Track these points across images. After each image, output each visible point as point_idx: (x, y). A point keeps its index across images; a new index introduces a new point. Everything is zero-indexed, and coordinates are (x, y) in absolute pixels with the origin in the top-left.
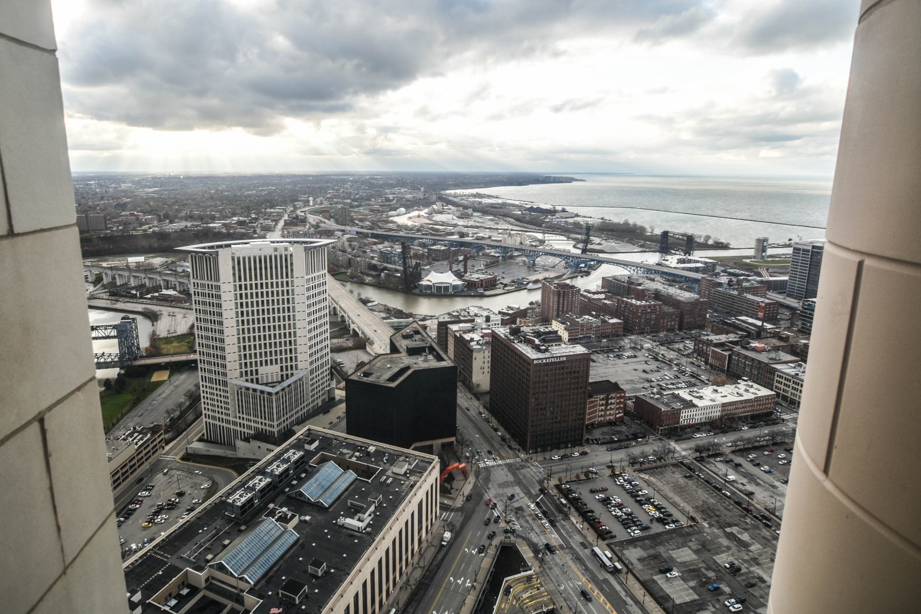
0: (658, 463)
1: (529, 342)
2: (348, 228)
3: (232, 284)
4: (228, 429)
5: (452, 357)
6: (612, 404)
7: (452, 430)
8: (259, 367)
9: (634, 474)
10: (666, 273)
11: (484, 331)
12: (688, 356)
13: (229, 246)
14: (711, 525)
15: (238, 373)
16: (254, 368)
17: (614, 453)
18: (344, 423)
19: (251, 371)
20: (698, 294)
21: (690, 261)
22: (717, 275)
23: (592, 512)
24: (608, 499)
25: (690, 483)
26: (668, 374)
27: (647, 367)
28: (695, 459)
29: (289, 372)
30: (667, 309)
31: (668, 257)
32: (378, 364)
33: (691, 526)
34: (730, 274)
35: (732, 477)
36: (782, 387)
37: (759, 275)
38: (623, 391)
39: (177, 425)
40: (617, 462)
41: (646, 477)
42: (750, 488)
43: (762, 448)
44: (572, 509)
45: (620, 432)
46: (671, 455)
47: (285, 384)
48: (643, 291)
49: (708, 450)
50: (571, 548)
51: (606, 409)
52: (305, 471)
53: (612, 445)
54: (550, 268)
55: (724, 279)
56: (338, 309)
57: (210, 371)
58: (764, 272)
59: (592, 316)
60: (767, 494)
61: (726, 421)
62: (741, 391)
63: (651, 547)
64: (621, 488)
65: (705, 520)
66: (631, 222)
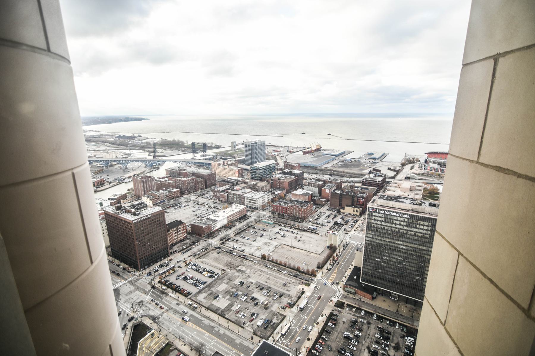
0: (206, 252)
10: (197, 163)
12: (211, 199)
21: (206, 156)
23: (179, 286)
25: (220, 255)
26: (204, 209)
27: (194, 209)
30: (199, 180)
31: (196, 155)
37: (234, 158)
38: (184, 223)
45: (186, 244)
46: (210, 246)
48: (186, 173)
53: (183, 251)
59: (164, 190)
62: (234, 209)
63: (209, 290)
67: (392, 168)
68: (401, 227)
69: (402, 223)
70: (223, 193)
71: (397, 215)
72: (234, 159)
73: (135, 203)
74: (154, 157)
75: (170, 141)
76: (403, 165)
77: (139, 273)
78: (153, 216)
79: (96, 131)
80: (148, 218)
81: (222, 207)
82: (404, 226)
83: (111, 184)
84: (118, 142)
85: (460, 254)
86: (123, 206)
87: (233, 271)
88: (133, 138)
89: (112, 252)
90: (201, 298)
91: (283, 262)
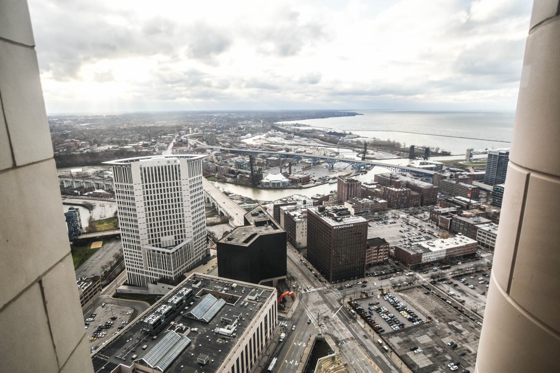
0: (409, 286)
1: (330, 216)
2: (214, 147)
3: (141, 184)
4: (143, 277)
5: (283, 227)
6: (381, 252)
7: (284, 272)
8: (161, 237)
9: (395, 293)
11: (303, 210)
12: (426, 221)
13: (138, 160)
14: (440, 321)
15: (147, 241)
16: (158, 238)
17: (383, 281)
18: (216, 270)
19: (156, 240)
20: (433, 183)
21: (427, 164)
22: (443, 171)
24: (379, 308)
25: (428, 297)
26: (415, 232)
27: (402, 229)
28: (431, 283)
29: (181, 239)
30: (414, 193)
31: (414, 161)
32: (237, 232)
33: (428, 322)
34: (451, 171)
35: (452, 292)
37: (468, 171)
38: (388, 244)
39: (109, 276)
40: (385, 287)
41: (402, 294)
42: (462, 298)
43: (469, 274)
44: (359, 317)
45: (386, 269)
46: (416, 281)
47: (178, 247)
48: (399, 182)
49: (438, 277)
50: (358, 339)
51: (378, 255)
52: (193, 301)
53: (382, 276)
55: (448, 174)
56: (210, 199)
57: (129, 241)
58: (471, 169)
59: (369, 199)
60: (472, 301)
61: (449, 259)
63: (405, 336)
64: (387, 302)
65: (437, 318)
70: (444, 217)
72: (468, 173)
74: (363, 159)
75: (384, 142)
77: (330, 286)
79: (309, 126)
80: (349, 228)
81: (440, 234)
84: (328, 139)
87: (443, 324)
88: (344, 135)
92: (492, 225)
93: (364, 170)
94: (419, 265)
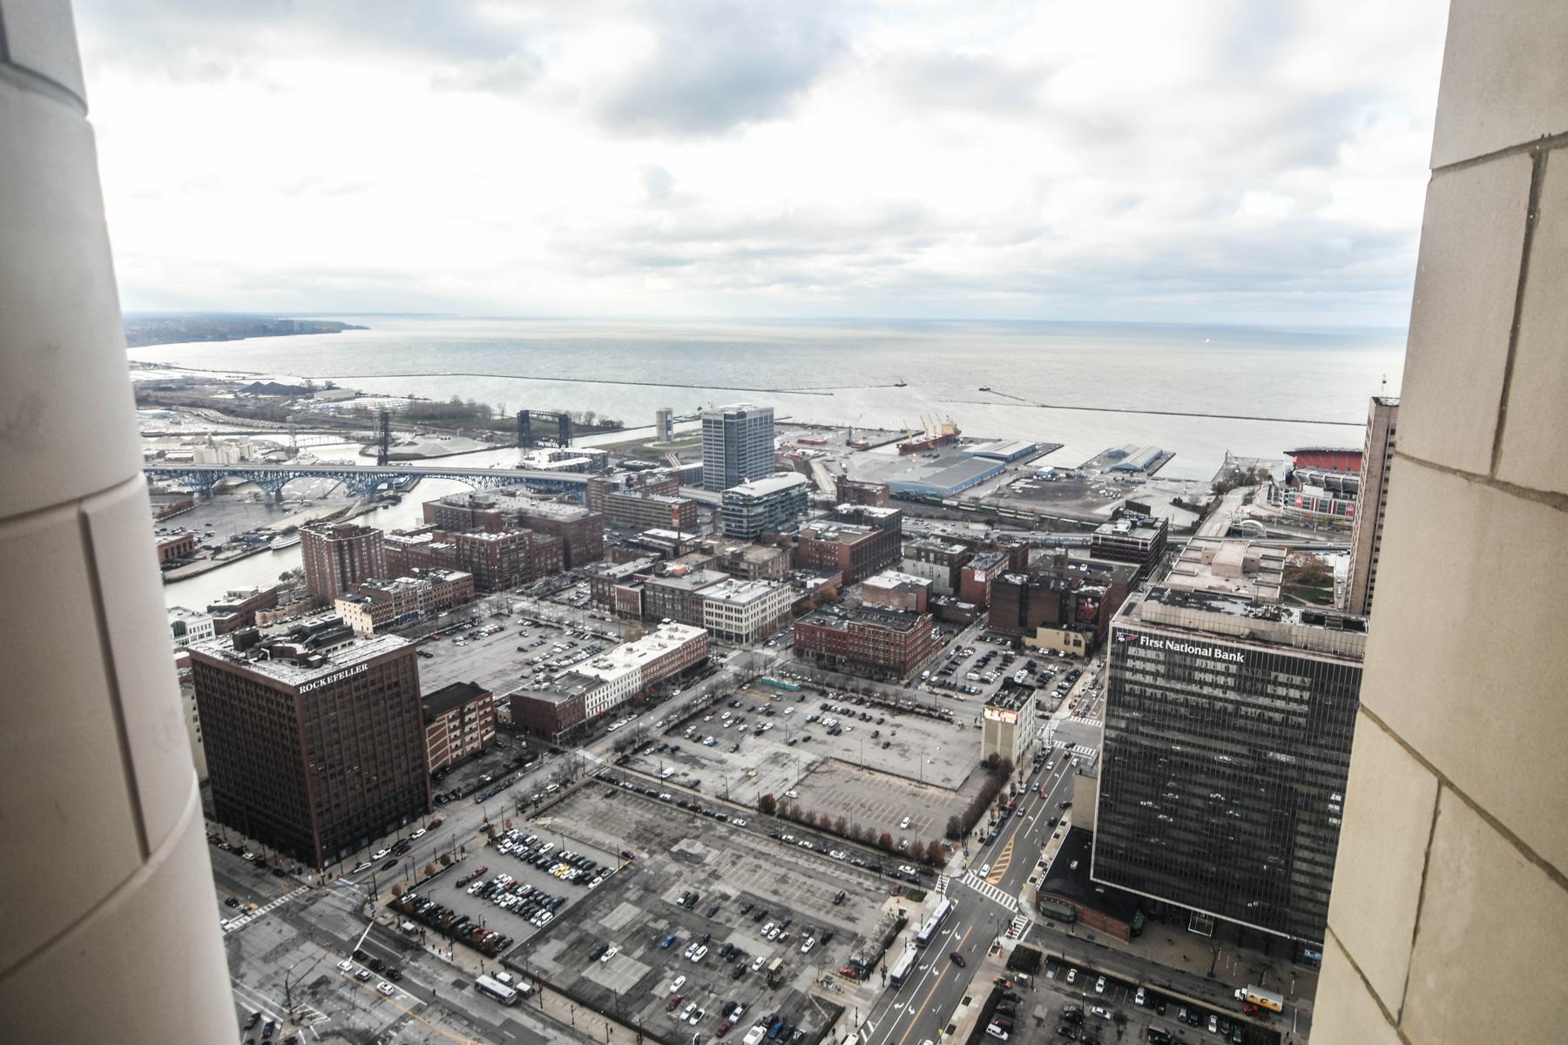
0: (564, 792)
6: (471, 721)
9: (529, 824)
17: (487, 803)
22: (610, 472)
26: (558, 643)
27: (523, 642)
28: (616, 763)
30: (542, 539)
31: (534, 453)
35: (669, 771)
36: (714, 619)
38: (488, 694)
40: (495, 817)
41: (547, 821)
42: (694, 776)
43: (701, 713)
45: (494, 765)
48: (498, 515)
49: (633, 742)
51: (463, 734)
53: (481, 791)
54: (314, 502)
55: (620, 478)
59: (414, 575)
60: (716, 774)
62: (664, 641)
66: (464, 401)
67: (1186, 500)
68: (1218, 693)
69: (1221, 680)
70: (625, 587)
71: (1205, 653)
73: (307, 622)
74: (383, 459)
75: (442, 405)
76: (1220, 490)
77: (318, 877)
78: (372, 670)
80: (355, 678)
82: (1225, 688)
83: (222, 556)
84: (251, 406)
85: (1443, 782)
86: (262, 633)
88: (308, 391)
89: (216, 802)
90: (545, 957)
91: (833, 820)
92: (730, 584)
93: (391, 493)
94: (582, 726)
